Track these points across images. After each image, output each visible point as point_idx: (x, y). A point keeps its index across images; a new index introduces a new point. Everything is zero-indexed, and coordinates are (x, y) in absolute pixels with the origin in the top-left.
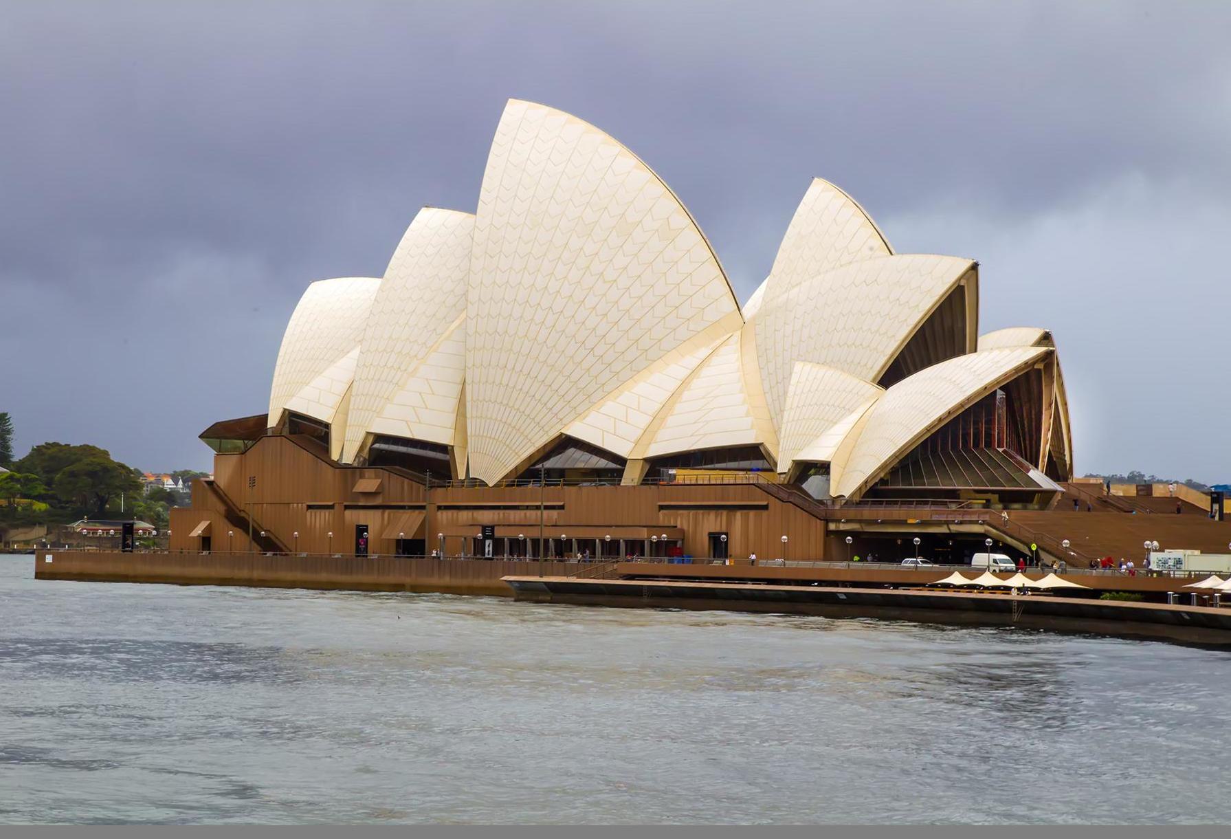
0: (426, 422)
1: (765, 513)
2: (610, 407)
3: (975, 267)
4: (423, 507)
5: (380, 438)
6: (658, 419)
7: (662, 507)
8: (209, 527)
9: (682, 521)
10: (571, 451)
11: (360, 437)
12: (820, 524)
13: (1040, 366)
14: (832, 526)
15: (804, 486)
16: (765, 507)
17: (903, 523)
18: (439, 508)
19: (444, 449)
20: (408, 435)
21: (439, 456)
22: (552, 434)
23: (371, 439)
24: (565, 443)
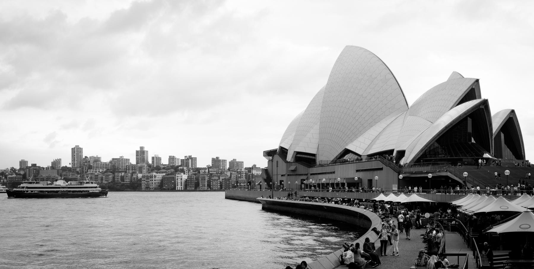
0: (308, 147)
1: (382, 171)
2: (361, 139)
5: (298, 153)
6: (373, 142)
7: (357, 171)
9: (361, 175)
11: (293, 152)
12: (397, 174)
16: (381, 169)
17: (422, 173)
18: (311, 174)
19: (314, 155)
20: (304, 151)
21: (313, 158)
22: (344, 149)
24: (347, 152)
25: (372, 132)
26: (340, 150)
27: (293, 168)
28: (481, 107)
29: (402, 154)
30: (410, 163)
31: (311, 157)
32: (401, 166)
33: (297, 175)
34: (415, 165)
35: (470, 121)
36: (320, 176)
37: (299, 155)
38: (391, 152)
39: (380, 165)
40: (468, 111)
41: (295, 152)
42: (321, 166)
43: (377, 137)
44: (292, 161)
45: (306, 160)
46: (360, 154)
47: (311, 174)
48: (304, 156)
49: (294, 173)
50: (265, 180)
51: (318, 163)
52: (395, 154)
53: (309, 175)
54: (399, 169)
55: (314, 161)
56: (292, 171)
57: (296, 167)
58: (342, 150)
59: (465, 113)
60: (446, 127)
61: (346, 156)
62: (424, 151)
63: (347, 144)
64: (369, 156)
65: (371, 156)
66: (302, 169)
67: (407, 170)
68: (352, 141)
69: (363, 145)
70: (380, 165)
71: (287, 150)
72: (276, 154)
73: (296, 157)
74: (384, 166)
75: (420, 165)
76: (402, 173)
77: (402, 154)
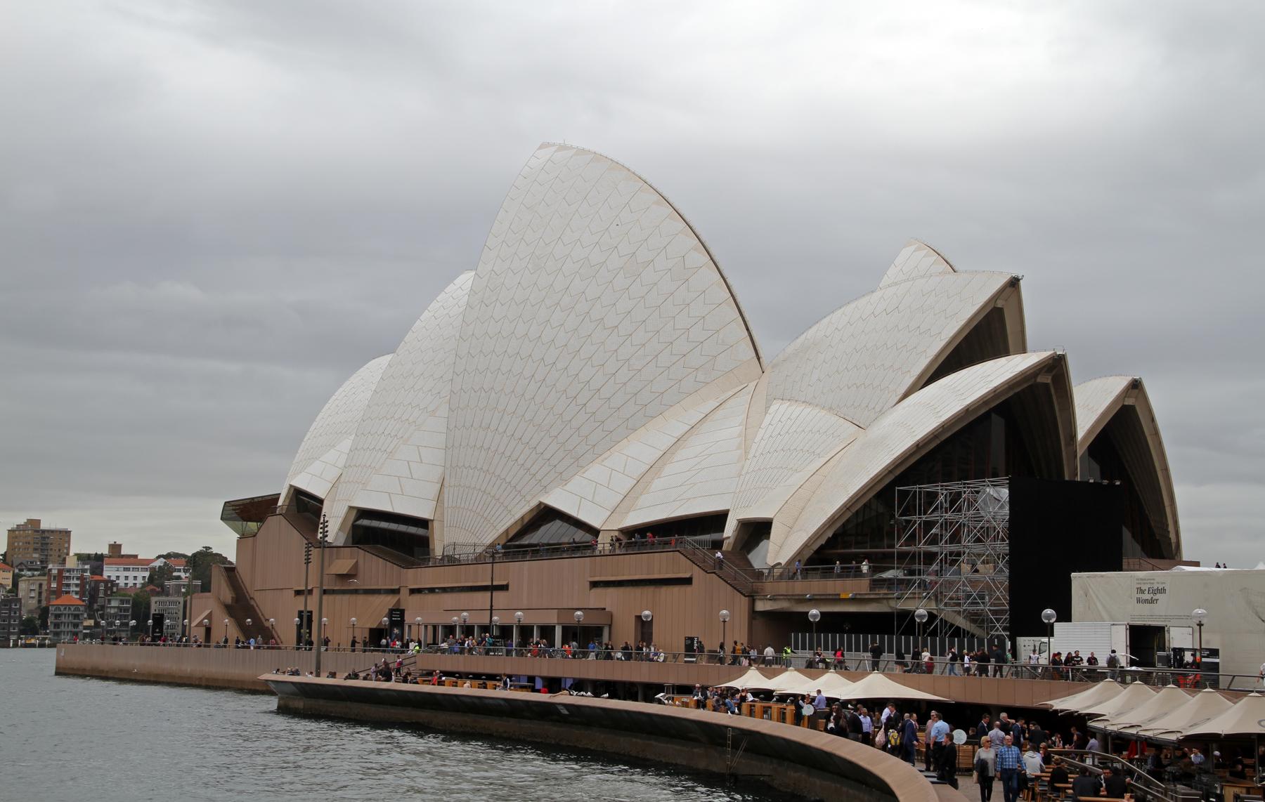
2: (595, 471)
3: (1014, 283)
4: (395, 592)
7: (594, 584)
8: (209, 617)
9: (608, 599)
10: (557, 524)
11: (345, 509)
13: (1047, 379)
14: (761, 606)
15: (749, 557)
16: (688, 581)
18: (413, 591)
19: (423, 523)
22: (534, 503)
23: (354, 512)
24: (546, 514)
25: (638, 450)
26: (521, 509)
27: (343, 565)
28: (1039, 380)
29: (757, 530)
30: (790, 562)
31: (412, 530)
32: (759, 575)
33: (356, 592)
34: (806, 573)
35: (998, 423)
36: (449, 600)
37: (366, 522)
38: (716, 520)
39: (683, 568)
40: (996, 393)
41: (351, 508)
42: (450, 561)
43: (655, 468)
44: (341, 542)
45: (394, 538)
46: (596, 524)
47: (413, 591)
48: (384, 525)
49: (345, 585)
50: (230, 610)
51: (438, 549)
52: (730, 529)
53: (404, 592)
54: (749, 582)
55: (424, 543)
56: (343, 577)
57: (356, 565)
58: (527, 509)
59: (984, 401)
60: (918, 446)
61: (543, 529)
62: (838, 524)
63: (545, 489)
64: (624, 531)
65: (640, 537)
66: (375, 568)
67: (783, 587)
68: (562, 479)
69: (603, 496)
70: (683, 568)
71: (321, 501)
72: (273, 513)
73: (355, 527)
74: (696, 573)
75: (827, 573)
76: (764, 598)
77: (757, 530)
